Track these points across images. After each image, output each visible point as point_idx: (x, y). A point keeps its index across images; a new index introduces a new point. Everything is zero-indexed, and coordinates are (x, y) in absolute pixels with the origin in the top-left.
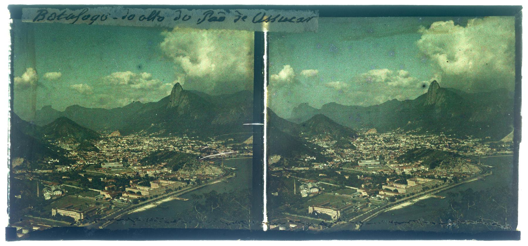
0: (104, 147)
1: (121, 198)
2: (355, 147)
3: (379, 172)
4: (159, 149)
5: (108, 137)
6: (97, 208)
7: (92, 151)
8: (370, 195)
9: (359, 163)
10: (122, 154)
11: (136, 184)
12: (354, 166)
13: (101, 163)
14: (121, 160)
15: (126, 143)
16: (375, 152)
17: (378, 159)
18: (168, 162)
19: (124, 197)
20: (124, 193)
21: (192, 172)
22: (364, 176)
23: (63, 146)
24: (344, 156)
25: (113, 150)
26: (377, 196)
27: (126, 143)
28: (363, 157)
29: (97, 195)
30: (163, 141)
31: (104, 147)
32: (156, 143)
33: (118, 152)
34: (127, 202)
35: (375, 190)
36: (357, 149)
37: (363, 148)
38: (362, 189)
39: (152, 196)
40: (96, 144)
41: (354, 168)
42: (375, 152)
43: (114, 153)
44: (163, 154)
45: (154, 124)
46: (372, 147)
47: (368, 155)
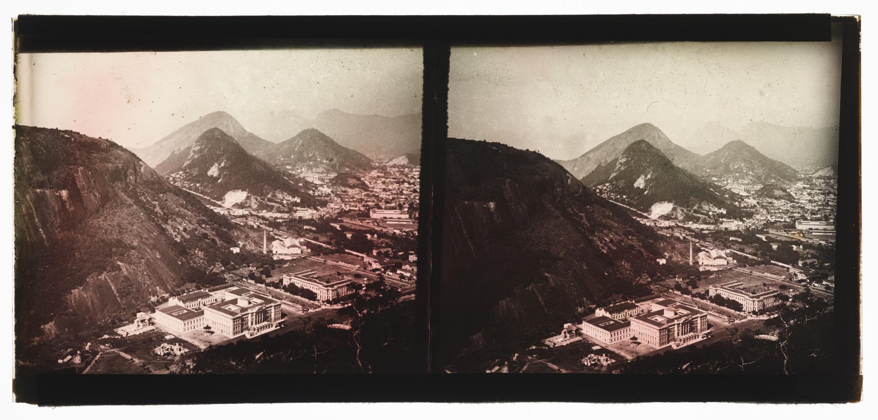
0: (378, 182)
1: (399, 272)
2: (793, 197)
3: (405, 232)
5: (811, 177)
8: (386, 269)
14: (406, 208)
16: (401, 197)
17: (406, 209)
22: (803, 247)
26: (399, 272)
28: (805, 215)
35: (395, 261)
37: (806, 200)
42: (401, 197)
43: (820, 205)
46: (397, 188)
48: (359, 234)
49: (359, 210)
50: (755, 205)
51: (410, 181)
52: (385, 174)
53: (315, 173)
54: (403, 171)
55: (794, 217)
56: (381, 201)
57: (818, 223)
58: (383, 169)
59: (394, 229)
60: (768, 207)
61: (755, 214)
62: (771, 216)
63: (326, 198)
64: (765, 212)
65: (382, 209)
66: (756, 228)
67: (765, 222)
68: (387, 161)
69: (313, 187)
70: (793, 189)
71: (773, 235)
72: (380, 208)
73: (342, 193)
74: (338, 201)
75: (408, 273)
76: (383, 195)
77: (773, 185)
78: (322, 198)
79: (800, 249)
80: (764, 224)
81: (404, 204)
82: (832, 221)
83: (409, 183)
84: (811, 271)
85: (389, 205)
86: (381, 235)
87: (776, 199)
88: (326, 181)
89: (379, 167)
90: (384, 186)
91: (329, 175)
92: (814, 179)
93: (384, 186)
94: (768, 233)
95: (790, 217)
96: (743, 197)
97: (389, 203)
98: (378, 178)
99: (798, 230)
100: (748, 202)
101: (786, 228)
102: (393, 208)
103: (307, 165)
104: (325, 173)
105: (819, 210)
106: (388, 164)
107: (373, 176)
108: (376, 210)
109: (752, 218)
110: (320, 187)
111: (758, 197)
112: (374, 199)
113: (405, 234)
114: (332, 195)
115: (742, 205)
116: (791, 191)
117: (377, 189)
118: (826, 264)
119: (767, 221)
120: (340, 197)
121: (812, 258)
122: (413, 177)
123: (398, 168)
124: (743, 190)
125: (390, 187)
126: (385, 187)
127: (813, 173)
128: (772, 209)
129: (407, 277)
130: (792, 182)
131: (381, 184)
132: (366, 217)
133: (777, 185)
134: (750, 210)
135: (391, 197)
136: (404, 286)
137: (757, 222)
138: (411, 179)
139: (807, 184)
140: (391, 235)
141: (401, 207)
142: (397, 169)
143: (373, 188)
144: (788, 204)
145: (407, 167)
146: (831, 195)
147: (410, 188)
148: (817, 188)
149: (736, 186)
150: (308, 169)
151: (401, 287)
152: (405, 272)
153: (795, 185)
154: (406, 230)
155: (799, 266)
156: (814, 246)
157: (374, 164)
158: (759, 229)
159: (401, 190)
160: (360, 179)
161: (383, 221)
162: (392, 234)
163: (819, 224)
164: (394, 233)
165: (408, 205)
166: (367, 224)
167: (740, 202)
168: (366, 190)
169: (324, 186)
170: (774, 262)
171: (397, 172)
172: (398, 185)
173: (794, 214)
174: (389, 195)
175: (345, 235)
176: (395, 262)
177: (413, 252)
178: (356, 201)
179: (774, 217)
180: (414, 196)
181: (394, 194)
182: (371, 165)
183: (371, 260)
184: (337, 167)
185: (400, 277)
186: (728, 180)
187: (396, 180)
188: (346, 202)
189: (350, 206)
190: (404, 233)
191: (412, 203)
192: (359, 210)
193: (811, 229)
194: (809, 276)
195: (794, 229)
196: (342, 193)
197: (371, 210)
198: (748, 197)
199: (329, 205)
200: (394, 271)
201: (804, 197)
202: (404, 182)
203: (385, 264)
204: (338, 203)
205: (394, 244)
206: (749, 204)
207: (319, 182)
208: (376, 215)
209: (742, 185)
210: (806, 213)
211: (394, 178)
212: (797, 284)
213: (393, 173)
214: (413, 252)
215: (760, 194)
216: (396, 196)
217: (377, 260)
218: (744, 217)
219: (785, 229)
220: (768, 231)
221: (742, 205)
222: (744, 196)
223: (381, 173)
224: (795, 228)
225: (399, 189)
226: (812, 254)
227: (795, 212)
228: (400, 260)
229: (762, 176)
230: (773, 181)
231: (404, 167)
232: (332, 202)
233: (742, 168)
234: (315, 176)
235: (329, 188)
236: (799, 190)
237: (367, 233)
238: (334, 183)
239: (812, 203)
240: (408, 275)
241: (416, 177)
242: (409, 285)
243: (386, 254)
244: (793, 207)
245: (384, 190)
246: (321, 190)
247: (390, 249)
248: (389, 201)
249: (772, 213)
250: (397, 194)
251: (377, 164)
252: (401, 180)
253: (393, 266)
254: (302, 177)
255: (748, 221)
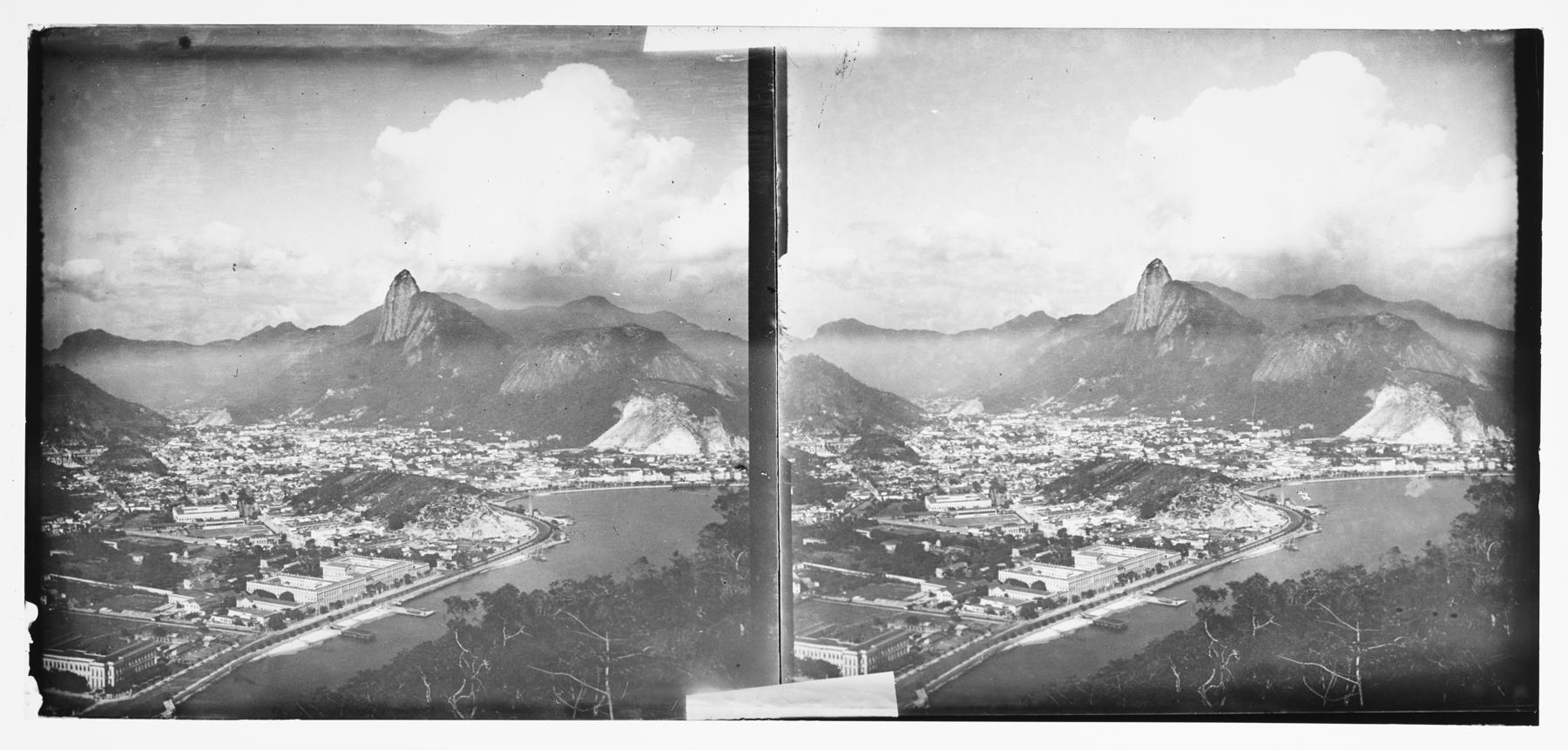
0: (182, 458)
3: (988, 530)
4: (348, 464)
5: (193, 429)
6: (158, 646)
7: (145, 470)
8: (961, 601)
9: (927, 502)
10: (237, 480)
11: (280, 570)
12: (912, 513)
13: (171, 507)
14: (234, 499)
15: (250, 447)
16: (976, 470)
17: (987, 491)
18: (374, 502)
19: (241, 609)
20: (243, 597)
21: (442, 530)
22: (942, 543)
23: (52, 456)
24: (882, 483)
25: (211, 468)
27: (250, 447)
28: (941, 485)
29: (158, 605)
30: (360, 440)
31: (182, 458)
32: (339, 446)
33: (224, 473)
34: (249, 625)
35: (975, 583)
36: (922, 460)
37: (941, 458)
38: (938, 582)
39: (326, 604)
40: (156, 450)
41: (911, 518)
42: (976, 470)
44: (361, 479)
45: (333, 390)
46: (968, 455)
47: (957, 479)
48: (909, 542)
49: (906, 499)
50: (847, 473)
51: (235, 454)
52: (193, 443)
53: (819, 436)
54: (974, 426)
55: (921, 489)
56: (942, 481)
57: (963, 497)
58: (940, 423)
59: (969, 527)
60: (873, 477)
61: (96, 502)
62: (880, 492)
63: (842, 483)
64: (867, 484)
65: (194, 505)
66: (853, 516)
67: (868, 503)
68: (947, 410)
69: (816, 463)
70: (163, 451)
71: (132, 538)
72: (189, 503)
73: (873, 471)
74: (112, 498)
75: (247, 614)
76: (946, 469)
77: (880, 436)
78: (836, 483)
79: (937, 547)
80: (868, 508)
81: (230, 493)
82: (235, 502)
83: (988, 446)
84: (959, 584)
85: (205, 497)
86: (949, 541)
87: (886, 461)
88: (840, 452)
89: (934, 419)
90: (946, 454)
91: (845, 440)
92: (951, 421)
93: (946, 454)
94: (123, 534)
95: (915, 491)
96: (824, 461)
97: (957, 483)
98: (181, 452)
99: (931, 513)
100: (82, 481)
101: (908, 512)
102: (965, 491)
103: (802, 424)
104: (837, 436)
105: (211, 486)
106: (197, 426)
107: (173, 448)
108: (184, 508)
109: (844, 499)
110: (829, 462)
111: (853, 459)
112: (929, 477)
113: (237, 545)
114: (854, 475)
115: (824, 476)
116: (160, 455)
117: (181, 470)
118: (983, 570)
119: (120, 514)
120: (116, 490)
121: (206, 572)
122: (240, 447)
123: (967, 420)
124: (823, 447)
125: (956, 455)
126: (194, 465)
127: (195, 421)
128: (881, 480)
129: (246, 620)
130: (159, 438)
131: (941, 450)
132: (919, 510)
133: (134, 445)
134: (86, 495)
135: (207, 483)
136: (996, 625)
137: (854, 505)
138: (989, 438)
139: (939, 430)
140: (966, 539)
141: (225, 498)
142: (965, 423)
143: (175, 469)
144: (908, 467)
145: (229, 429)
146: (228, 458)
147: (989, 454)
148: (957, 436)
149: (56, 451)
150: (804, 431)
151: (990, 630)
152: (242, 611)
153: (919, 433)
154: (238, 539)
155: (186, 590)
156: (959, 539)
157: (925, 416)
158: (858, 517)
159: (974, 458)
160: (151, 455)
161: (948, 514)
162: (216, 548)
163: (213, 510)
164: (971, 534)
165: (990, 483)
166: (168, 534)
167: (818, 470)
168: (917, 463)
169: (838, 459)
170: (891, 576)
171: (966, 428)
172: (969, 450)
173: (920, 485)
174: (955, 469)
175: (884, 547)
176: (976, 586)
177: (1004, 565)
178: (899, 484)
179: (133, 505)
180: (245, 479)
181: (965, 466)
182: (921, 417)
183: (934, 588)
184: (107, 434)
185: (985, 611)
186: (792, 430)
187: (966, 442)
188: (128, 497)
189: (889, 493)
190: (986, 533)
191: (995, 479)
192: (906, 499)
193: (953, 509)
194: (958, 593)
195: (921, 513)
196: (873, 471)
197: (926, 497)
198: (833, 460)
199: (849, 495)
200: (223, 613)
201: (184, 464)
202: (226, 455)
203: (960, 591)
204: (113, 501)
205: (972, 553)
206: (837, 472)
207: (827, 454)
208: (937, 505)
209: (820, 438)
210: (190, 492)
211: (211, 450)
212: (937, 610)
213: (958, 430)
214: (252, 576)
215: (854, 454)
216: (967, 470)
217: (192, 598)
218: (830, 498)
219: (907, 514)
220: (123, 532)
221: (70, 486)
222: (826, 458)
223: (187, 441)
224: (923, 509)
225: (971, 457)
226: (959, 554)
227: (171, 492)
228: (231, 594)
229: (105, 430)
230: (879, 427)
231: (223, 429)
232: (854, 490)
233: (819, 407)
234: (818, 444)
235: (848, 464)
236: (925, 441)
237: (172, 551)
238: (103, 466)
239: (950, 463)
240: (248, 616)
241: (245, 446)
242: (1002, 623)
243: (960, 574)
244: (165, 484)
245: (947, 460)
246: (79, 478)
247: (965, 564)
248: (205, 490)
249: (881, 486)
250: (217, 477)
251: (930, 416)
252: (974, 441)
253: (972, 595)
254: (793, 446)
255: (836, 504)
